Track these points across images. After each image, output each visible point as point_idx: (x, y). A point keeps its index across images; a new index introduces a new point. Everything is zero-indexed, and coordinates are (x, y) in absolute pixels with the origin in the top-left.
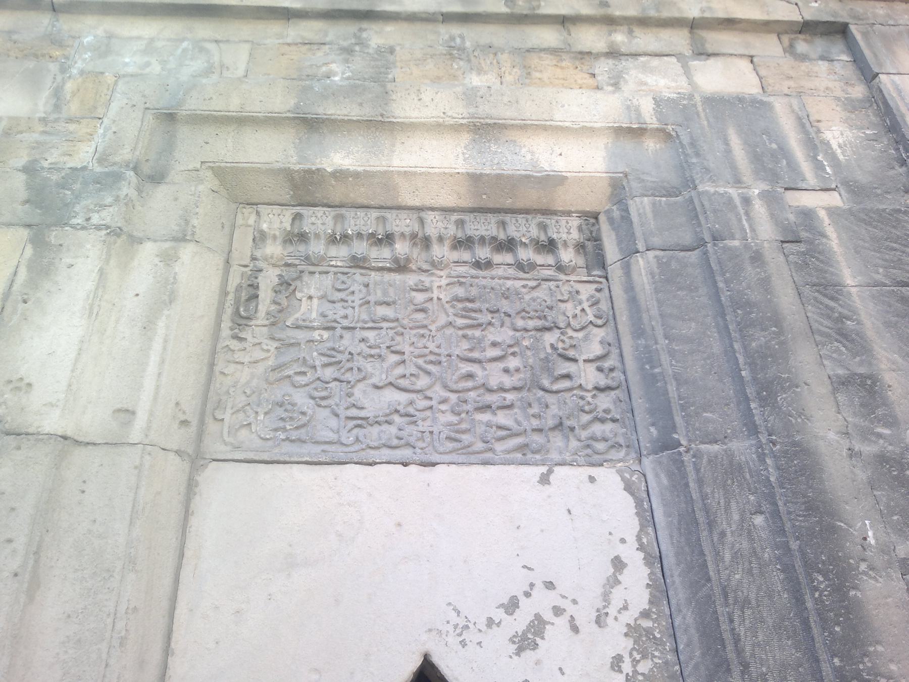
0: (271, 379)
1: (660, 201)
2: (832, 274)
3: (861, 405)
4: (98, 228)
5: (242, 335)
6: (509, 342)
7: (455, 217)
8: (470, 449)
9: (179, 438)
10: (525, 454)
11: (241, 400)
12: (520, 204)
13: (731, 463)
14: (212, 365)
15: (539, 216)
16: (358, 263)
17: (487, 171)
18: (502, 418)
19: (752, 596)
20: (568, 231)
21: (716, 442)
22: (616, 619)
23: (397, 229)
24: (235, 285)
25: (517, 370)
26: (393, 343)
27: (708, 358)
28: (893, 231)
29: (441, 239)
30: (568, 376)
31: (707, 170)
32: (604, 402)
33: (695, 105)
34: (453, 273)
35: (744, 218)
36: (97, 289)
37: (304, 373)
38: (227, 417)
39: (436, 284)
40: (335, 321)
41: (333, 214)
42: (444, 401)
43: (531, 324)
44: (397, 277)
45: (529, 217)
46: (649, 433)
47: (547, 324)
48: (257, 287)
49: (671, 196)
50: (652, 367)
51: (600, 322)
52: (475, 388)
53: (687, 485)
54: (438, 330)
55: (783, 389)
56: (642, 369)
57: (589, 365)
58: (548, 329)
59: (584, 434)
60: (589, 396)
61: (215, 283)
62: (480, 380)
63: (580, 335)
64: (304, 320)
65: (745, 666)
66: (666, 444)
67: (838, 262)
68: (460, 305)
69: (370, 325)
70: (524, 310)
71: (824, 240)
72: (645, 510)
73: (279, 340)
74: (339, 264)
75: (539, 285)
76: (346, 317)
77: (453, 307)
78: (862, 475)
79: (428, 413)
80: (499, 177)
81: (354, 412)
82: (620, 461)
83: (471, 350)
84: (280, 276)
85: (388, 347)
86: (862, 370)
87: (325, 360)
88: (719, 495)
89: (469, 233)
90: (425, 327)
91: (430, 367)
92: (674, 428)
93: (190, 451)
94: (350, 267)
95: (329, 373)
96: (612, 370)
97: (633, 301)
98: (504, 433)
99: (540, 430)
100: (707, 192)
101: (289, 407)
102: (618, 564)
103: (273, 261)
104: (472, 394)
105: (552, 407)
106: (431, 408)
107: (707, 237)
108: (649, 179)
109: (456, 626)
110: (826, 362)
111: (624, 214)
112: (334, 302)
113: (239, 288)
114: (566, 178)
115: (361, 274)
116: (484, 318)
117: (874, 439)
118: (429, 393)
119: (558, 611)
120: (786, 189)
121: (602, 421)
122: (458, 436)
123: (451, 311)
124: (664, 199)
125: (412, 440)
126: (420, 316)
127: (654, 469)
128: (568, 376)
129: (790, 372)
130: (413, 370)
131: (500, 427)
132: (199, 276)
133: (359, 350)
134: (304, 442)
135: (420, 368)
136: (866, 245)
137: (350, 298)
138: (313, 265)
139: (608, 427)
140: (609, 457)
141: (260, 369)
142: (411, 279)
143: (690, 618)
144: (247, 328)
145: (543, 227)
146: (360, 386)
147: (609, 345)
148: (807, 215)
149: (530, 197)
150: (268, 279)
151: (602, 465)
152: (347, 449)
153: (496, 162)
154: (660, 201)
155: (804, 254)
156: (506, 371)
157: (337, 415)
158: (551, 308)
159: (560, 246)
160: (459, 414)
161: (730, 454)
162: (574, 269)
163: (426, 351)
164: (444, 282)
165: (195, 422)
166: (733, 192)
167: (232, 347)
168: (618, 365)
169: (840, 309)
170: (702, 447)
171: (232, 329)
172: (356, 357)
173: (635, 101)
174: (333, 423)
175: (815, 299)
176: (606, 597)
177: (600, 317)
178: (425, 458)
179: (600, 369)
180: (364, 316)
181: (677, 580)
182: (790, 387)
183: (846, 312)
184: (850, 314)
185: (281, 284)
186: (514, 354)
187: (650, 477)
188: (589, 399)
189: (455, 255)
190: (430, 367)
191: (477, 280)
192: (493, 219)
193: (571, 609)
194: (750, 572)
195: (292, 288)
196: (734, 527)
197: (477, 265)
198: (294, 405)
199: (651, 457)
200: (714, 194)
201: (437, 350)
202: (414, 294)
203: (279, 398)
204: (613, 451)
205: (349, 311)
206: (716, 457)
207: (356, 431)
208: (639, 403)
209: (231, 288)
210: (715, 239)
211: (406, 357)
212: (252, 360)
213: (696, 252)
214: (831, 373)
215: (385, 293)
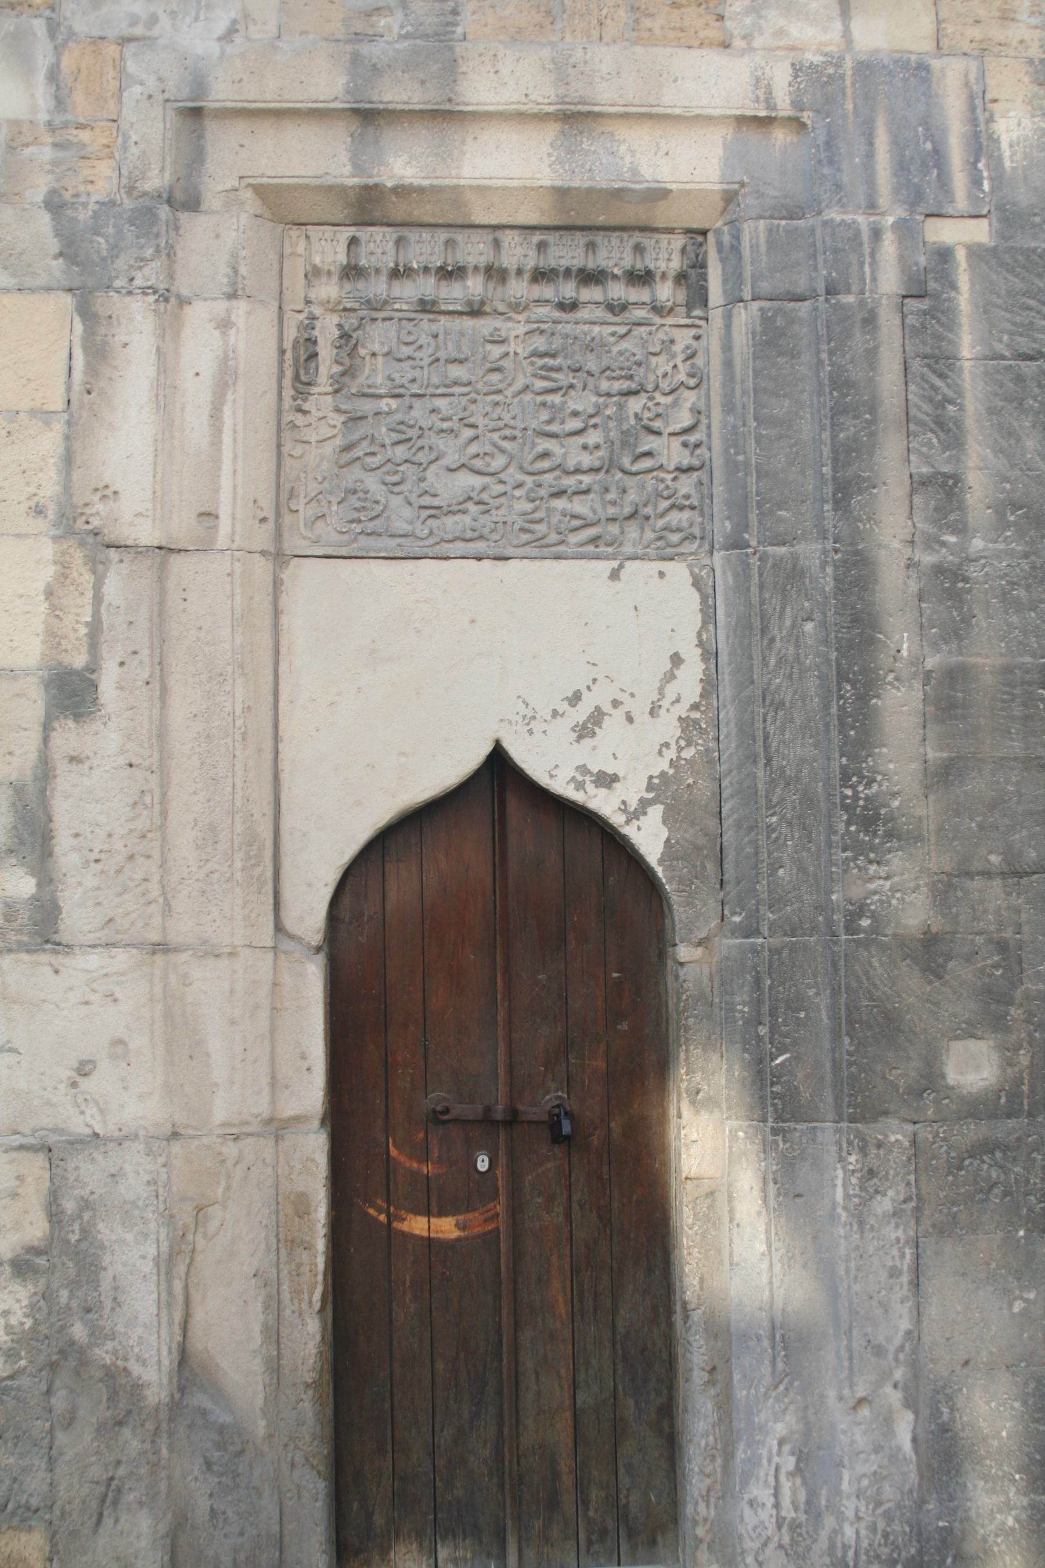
0: (342, 462)
1: (778, 226)
2: (950, 342)
3: (936, 509)
4: (145, 291)
5: (306, 407)
6: (591, 410)
7: (537, 238)
8: (542, 542)
9: (262, 537)
10: (597, 546)
11: (313, 488)
12: (613, 222)
13: (794, 568)
14: (279, 446)
15: (637, 233)
16: (427, 307)
17: (576, 184)
18: (580, 506)
19: (788, 699)
20: (667, 256)
21: (784, 544)
22: (668, 710)
23: (470, 259)
24: (292, 338)
25: (597, 447)
26: (466, 414)
27: (796, 444)
28: (1037, 281)
29: (519, 272)
30: (648, 454)
31: (838, 187)
32: (686, 485)
33: (842, 77)
34: (533, 317)
35: (868, 260)
36: (158, 374)
37: (373, 454)
38: (301, 508)
39: (514, 333)
40: (402, 386)
41: (395, 236)
42: (519, 486)
44: (468, 323)
45: (625, 235)
46: (722, 527)
47: (634, 386)
48: (315, 342)
49: (791, 218)
50: (737, 453)
51: (692, 382)
52: (551, 470)
53: (748, 589)
54: (513, 397)
55: (860, 491)
56: (726, 451)
57: (673, 438)
58: (635, 393)
59: (660, 523)
60: (670, 476)
61: (272, 345)
63: (669, 399)
64: (369, 387)
65: (769, 760)
66: (736, 543)
67: (960, 325)
68: (540, 362)
69: (440, 391)
70: (608, 368)
71: (953, 294)
72: (709, 607)
73: (345, 412)
74: (405, 307)
75: (630, 331)
76: (414, 380)
77: (532, 364)
78: (914, 587)
79: (503, 500)
80: (590, 191)
81: (427, 500)
82: (692, 554)
83: (549, 422)
84: (340, 326)
86: (946, 469)
87: (396, 437)
88: (776, 602)
89: (553, 263)
90: (499, 392)
91: (505, 444)
92: (746, 528)
93: (272, 550)
96: (697, 446)
97: (728, 364)
98: (576, 523)
99: (613, 520)
100: (832, 220)
101: (361, 495)
102: (676, 660)
103: (330, 306)
104: (548, 477)
105: (631, 491)
106: (505, 493)
107: (821, 288)
108: (772, 193)
109: (524, 717)
110: (912, 457)
111: (735, 243)
112: (400, 360)
113: (296, 342)
114: (671, 191)
115: (430, 320)
116: (563, 378)
117: (937, 547)
118: (503, 476)
119: (616, 704)
120: (927, 216)
121: (681, 508)
122: (532, 526)
123: (529, 370)
124: (783, 222)
125: (486, 531)
126: (495, 377)
127: (723, 566)
128: (648, 454)
129: (871, 470)
130: (488, 448)
131: (574, 517)
132: (256, 338)
133: (430, 424)
134: (380, 535)
135: (495, 445)
136: (1000, 301)
137: (418, 355)
138: (375, 309)
139: (686, 515)
140: (681, 550)
141: (328, 449)
142: (485, 326)
143: (732, 714)
144: (311, 398)
145: (639, 249)
146: (433, 468)
147: (699, 413)
148: (944, 255)
149: (629, 214)
150: (327, 330)
151: (672, 559)
152: (421, 544)
153: (587, 167)
154: (778, 226)
155: (925, 313)
156: (585, 447)
157: (410, 504)
158: (639, 364)
159: (658, 279)
160: (533, 501)
161: (795, 558)
163: (501, 424)
164: (521, 330)
165: (272, 517)
166: (862, 220)
167: (298, 423)
168: (704, 438)
169: (946, 390)
170: (769, 548)
171: (295, 400)
172: (427, 433)
173: (767, 70)
174: (407, 512)
175: (923, 377)
176: (661, 691)
177: (691, 375)
179: (685, 445)
180: (435, 380)
181: (727, 678)
182: (867, 488)
183: (951, 394)
184: (955, 396)
185: (341, 337)
186: (595, 426)
187: (718, 573)
188: (669, 483)
190: (505, 444)
191: (560, 326)
192: (581, 239)
193: (629, 704)
194: (790, 676)
195: (354, 341)
196: (784, 633)
197: (562, 306)
198: (367, 492)
199: (722, 553)
200: (840, 224)
201: (512, 423)
202: (489, 347)
203: (351, 486)
205: (417, 373)
206: (781, 560)
207: (430, 522)
208: (718, 489)
209: (288, 345)
210: (828, 292)
211: (479, 431)
212: (320, 438)
213: (806, 303)
214: (914, 471)
215: (459, 347)
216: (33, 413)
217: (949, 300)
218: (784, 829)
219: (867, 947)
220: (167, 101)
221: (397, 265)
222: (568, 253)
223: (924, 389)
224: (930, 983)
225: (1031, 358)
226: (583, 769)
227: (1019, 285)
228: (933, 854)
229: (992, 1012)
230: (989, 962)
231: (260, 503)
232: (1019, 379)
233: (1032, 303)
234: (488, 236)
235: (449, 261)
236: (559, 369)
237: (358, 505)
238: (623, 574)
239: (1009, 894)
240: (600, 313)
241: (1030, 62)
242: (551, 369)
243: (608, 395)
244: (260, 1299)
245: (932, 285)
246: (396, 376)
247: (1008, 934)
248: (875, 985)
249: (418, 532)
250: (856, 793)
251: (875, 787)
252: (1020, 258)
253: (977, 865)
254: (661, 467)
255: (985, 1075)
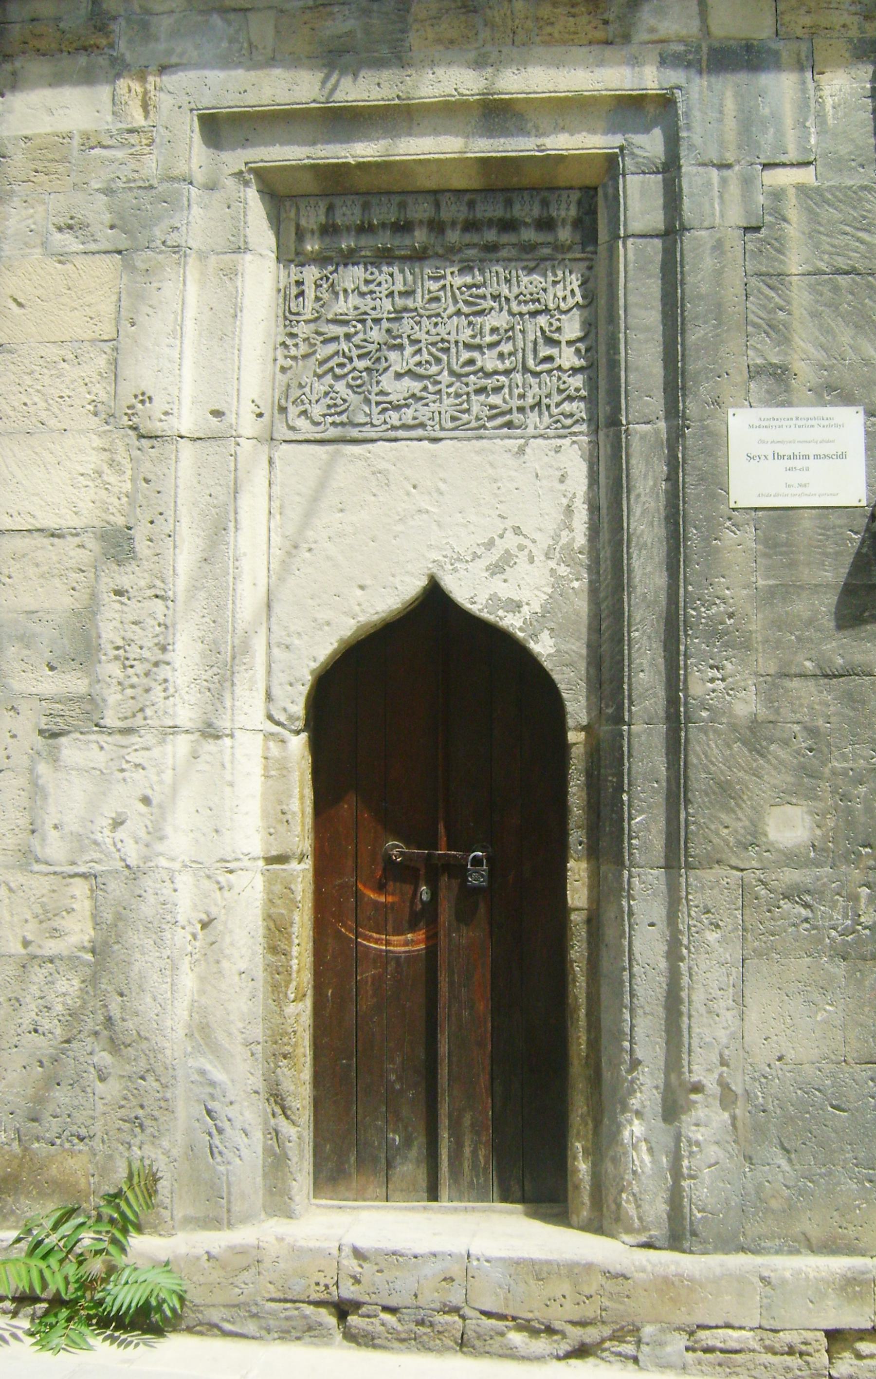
5: (295, 330)
6: (506, 326)
12: (525, 182)
21: (649, 423)
40: (366, 313)
43: (524, 309)
48: (302, 283)
52: (475, 373)
62: (479, 364)
71: (785, 225)
74: (369, 254)
76: (374, 309)
83: (473, 337)
85: (409, 336)
89: (479, 215)
90: (438, 315)
94: (377, 257)
95: (361, 364)
99: (521, 410)
110: (750, 352)
118: (438, 378)
119: (521, 548)
120: (766, 166)
124: (653, 176)
126: (434, 305)
131: (492, 407)
143: (608, 555)
148: (777, 195)
162: (570, 248)
178: (433, 434)
181: (606, 525)
182: (712, 377)
189: (468, 238)
196: (648, 491)
204: (577, 425)
209: (282, 286)
214: (751, 363)
216: (92, 341)
217: (781, 229)
218: (645, 641)
219: (706, 733)
220: (192, 110)
221: (363, 223)
222: (492, 210)
223: (759, 299)
224: (755, 760)
225: (847, 273)
226: (494, 597)
227: (838, 216)
228: (760, 660)
229: (805, 782)
230: (803, 745)
231: (257, 402)
232: (836, 289)
233: (848, 229)
234: (431, 199)
235: (402, 217)
236: (484, 297)
237: (331, 402)
238: (528, 450)
239: (821, 692)
240: (514, 252)
241: (850, 40)
242: (477, 297)
243: (521, 314)
244: (248, 990)
245: (768, 218)
246: (361, 306)
247: (820, 722)
248: (712, 763)
249: (375, 422)
250: (699, 613)
251: (714, 609)
252: (838, 193)
253: (794, 670)
254: (559, 368)
255: (799, 833)
